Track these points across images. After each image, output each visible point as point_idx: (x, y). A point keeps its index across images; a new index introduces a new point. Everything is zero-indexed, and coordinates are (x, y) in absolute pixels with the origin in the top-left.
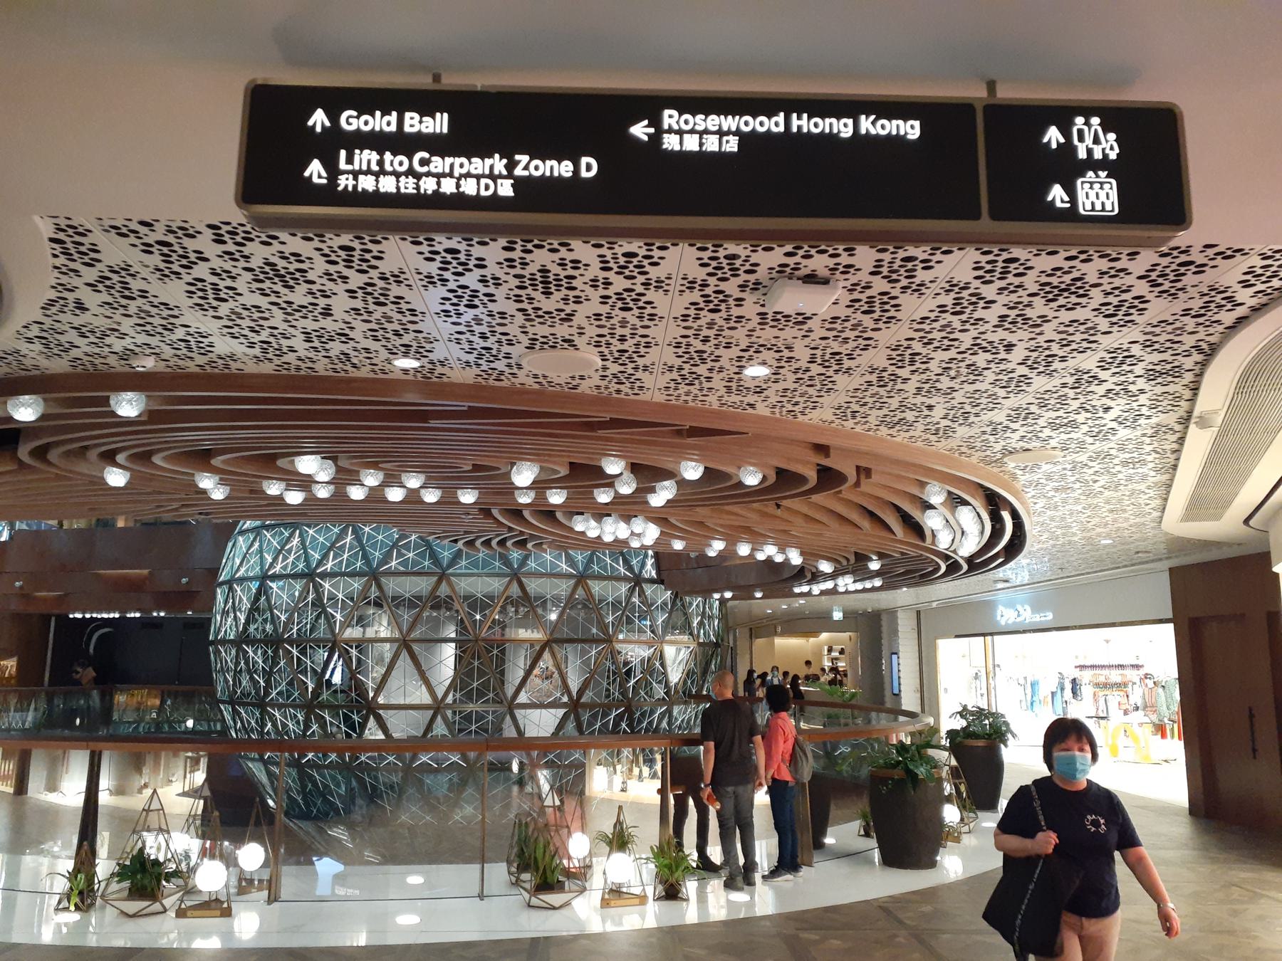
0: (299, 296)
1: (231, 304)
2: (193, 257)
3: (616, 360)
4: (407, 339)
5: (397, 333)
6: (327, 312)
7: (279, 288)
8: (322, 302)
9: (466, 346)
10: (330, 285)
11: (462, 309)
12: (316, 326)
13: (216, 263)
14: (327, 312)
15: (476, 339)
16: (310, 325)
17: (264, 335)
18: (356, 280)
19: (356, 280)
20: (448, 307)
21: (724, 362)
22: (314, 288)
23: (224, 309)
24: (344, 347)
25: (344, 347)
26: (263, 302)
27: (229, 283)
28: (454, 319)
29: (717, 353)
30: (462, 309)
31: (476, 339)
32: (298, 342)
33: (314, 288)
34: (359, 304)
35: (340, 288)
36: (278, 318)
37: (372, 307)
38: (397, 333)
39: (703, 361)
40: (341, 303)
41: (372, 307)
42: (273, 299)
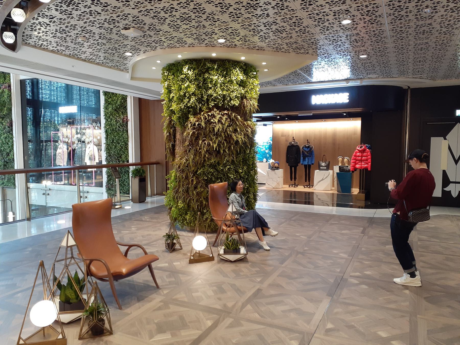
0: (284, 35)
1: (269, 39)
2: (260, 31)
3: (374, 37)
4: (312, 41)
5: (309, 40)
6: (291, 37)
7: (279, 34)
8: (290, 35)
9: (329, 40)
10: (291, 31)
11: (325, 31)
12: (289, 41)
13: (265, 31)
14: (291, 37)
15: (331, 37)
16: (287, 41)
17: (277, 45)
18: (297, 29)
19: (297, 29)
20: (321, 31)
21: (410, 32)
22: (288, 32)
23: (267, 41)
24: (296, 45)
25: (296, 45)
26: (276, 38)
27: (268, 35)
28: (324, 34)
29: (407, 30)
30: (325, 31)
31: (331, 37)
32: (285, 46)
33: (288, 32)
34: (299, 34)
35: (294, 31)
36: (279, 41)
37: (302, 34)
38: (309, 40)
39: (403, 33)
40: (294, 35)
41: (302, 34)
42: (278, 37)
